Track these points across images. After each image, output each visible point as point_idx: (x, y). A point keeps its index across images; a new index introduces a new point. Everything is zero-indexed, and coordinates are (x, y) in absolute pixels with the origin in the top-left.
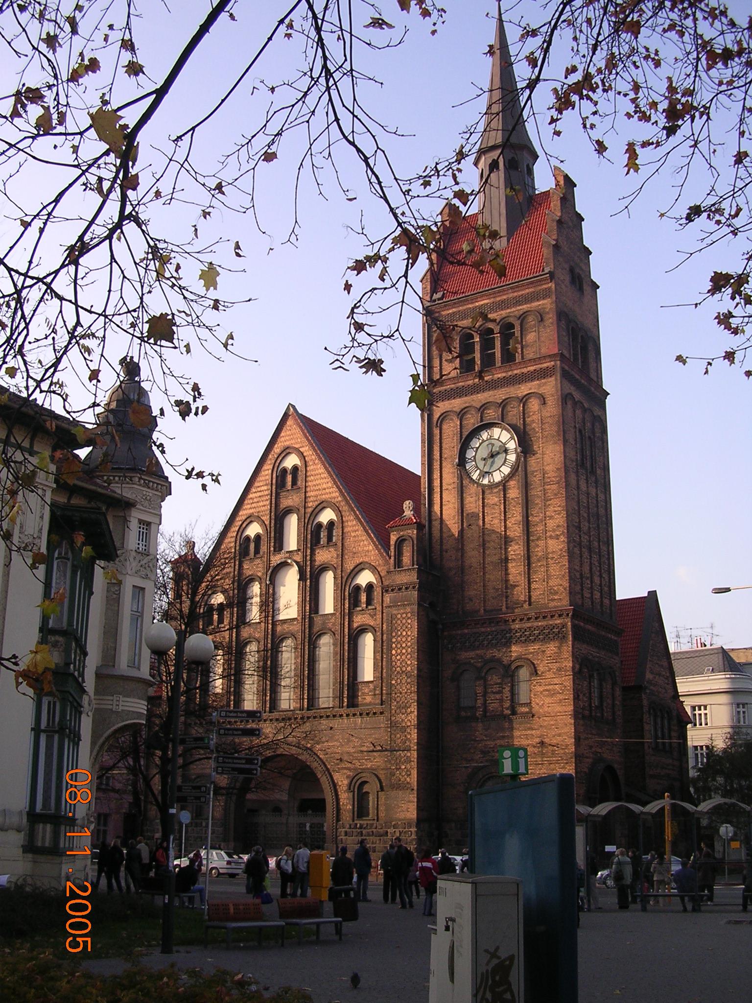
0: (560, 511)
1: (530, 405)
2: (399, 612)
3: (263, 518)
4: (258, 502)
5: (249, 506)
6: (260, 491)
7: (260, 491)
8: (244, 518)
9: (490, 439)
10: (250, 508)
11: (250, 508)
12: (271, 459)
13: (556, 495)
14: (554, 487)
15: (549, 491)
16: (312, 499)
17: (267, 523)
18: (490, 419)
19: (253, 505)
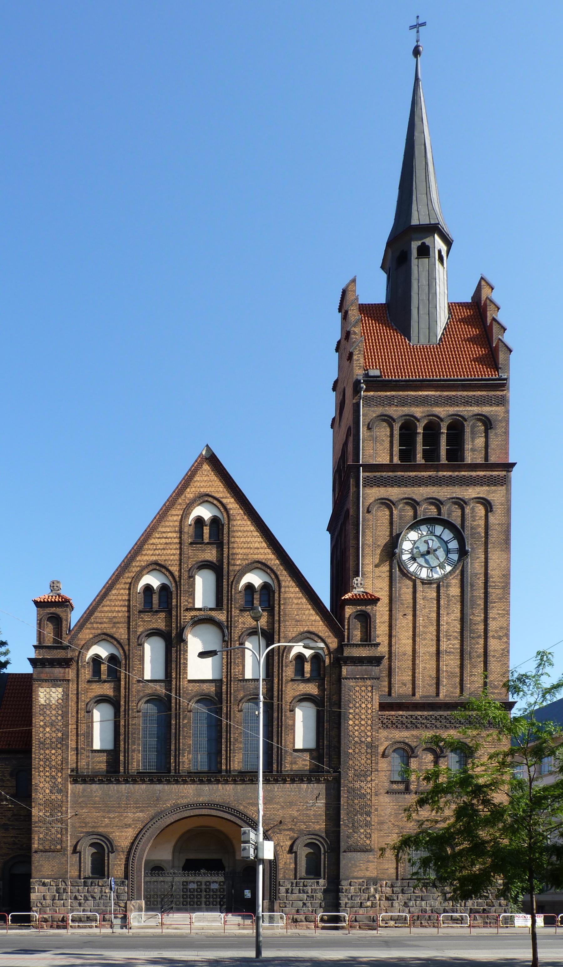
0: (504, 614)
1: (477, 510)
2: (358, 684)
3: (171, 568)
4: (164, 549)
5: (151, 552)
6: (166, 538)
7: (166, 538)
8: (143, 564)
9: (421, 537)
10: (153, 555)
11: (153, 555)
12: (180, 504)
13: (500, 599)
14: (499, 591)
15: (494, 595)
16: (239, 556)
17: (176, 574)
18: (430, 515)
19: (157, 552)
